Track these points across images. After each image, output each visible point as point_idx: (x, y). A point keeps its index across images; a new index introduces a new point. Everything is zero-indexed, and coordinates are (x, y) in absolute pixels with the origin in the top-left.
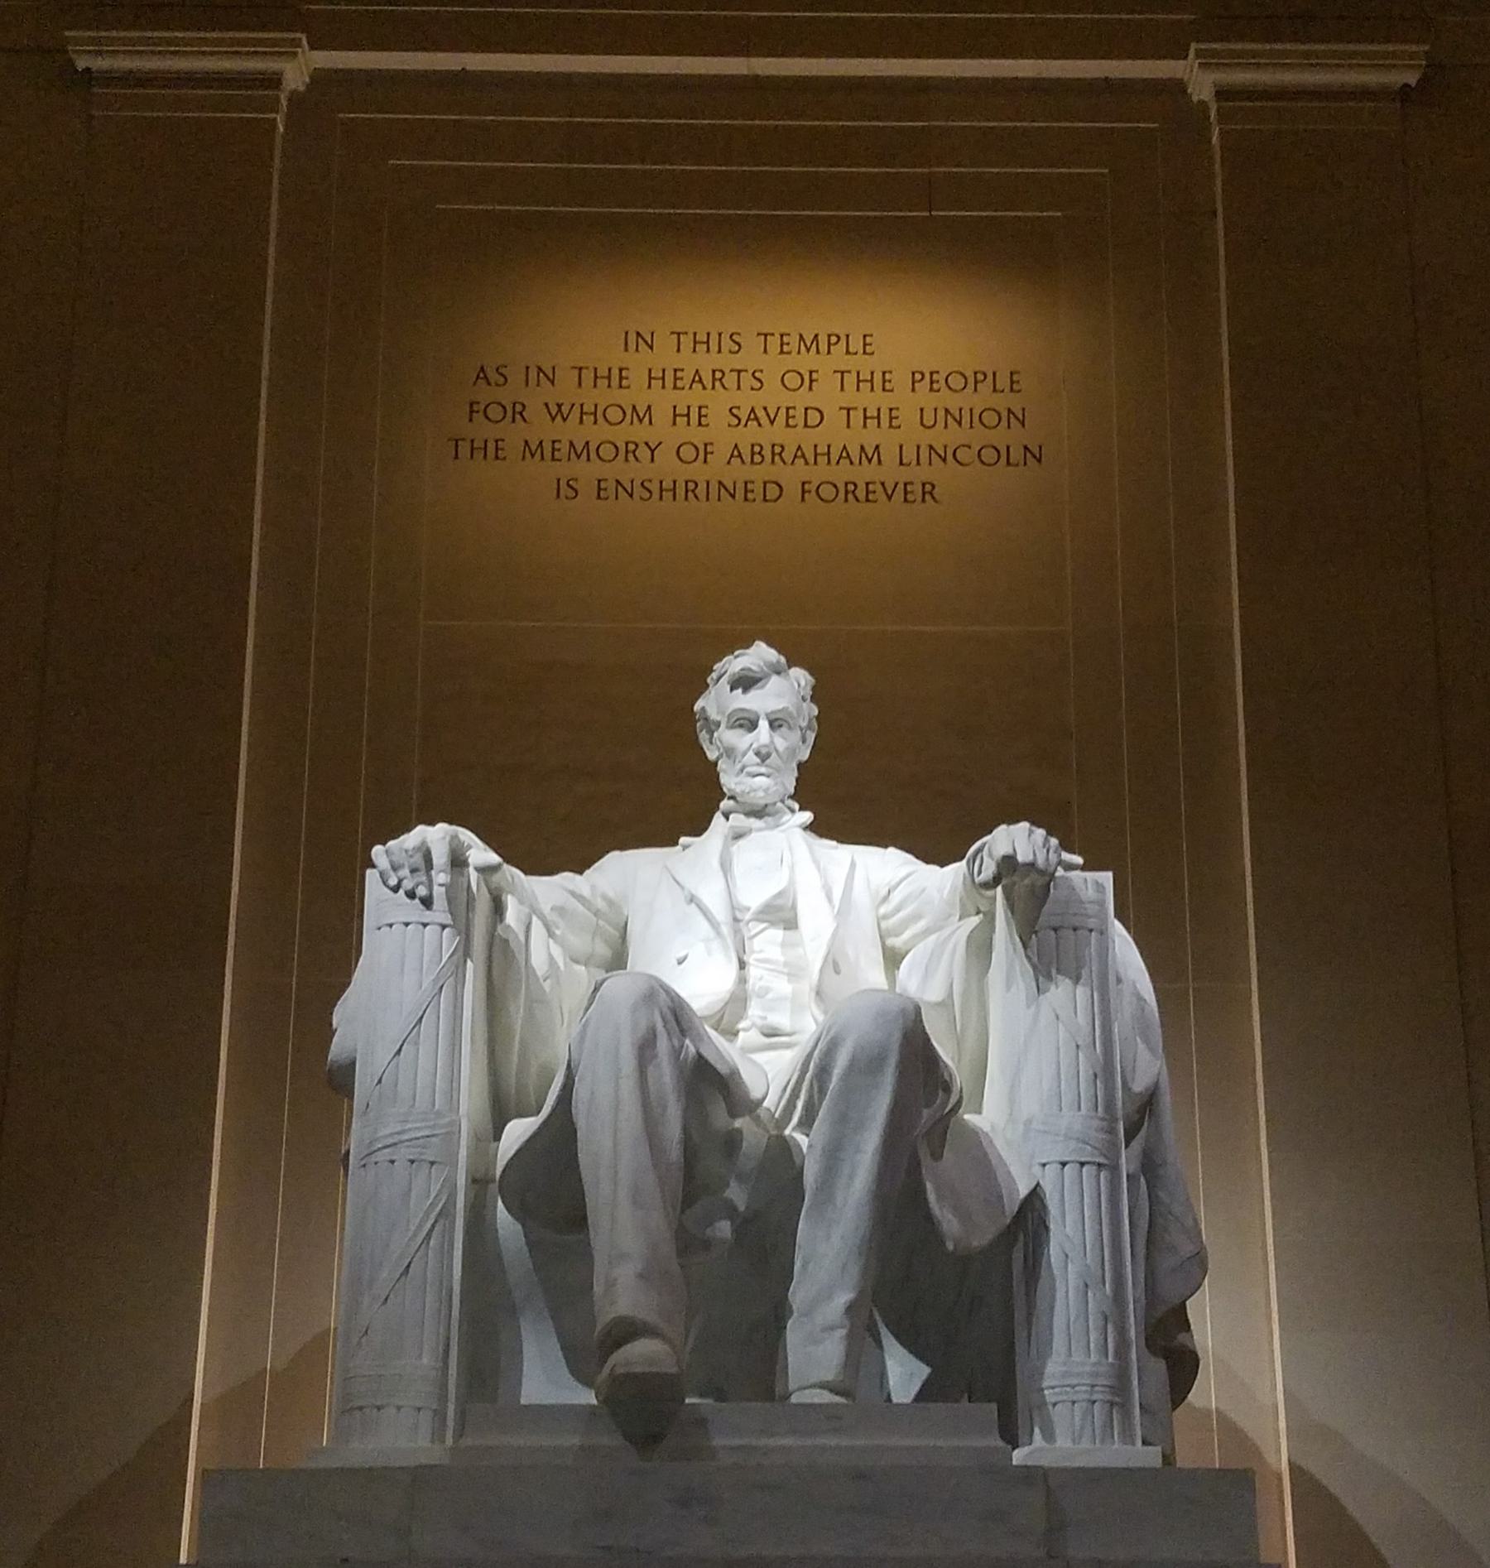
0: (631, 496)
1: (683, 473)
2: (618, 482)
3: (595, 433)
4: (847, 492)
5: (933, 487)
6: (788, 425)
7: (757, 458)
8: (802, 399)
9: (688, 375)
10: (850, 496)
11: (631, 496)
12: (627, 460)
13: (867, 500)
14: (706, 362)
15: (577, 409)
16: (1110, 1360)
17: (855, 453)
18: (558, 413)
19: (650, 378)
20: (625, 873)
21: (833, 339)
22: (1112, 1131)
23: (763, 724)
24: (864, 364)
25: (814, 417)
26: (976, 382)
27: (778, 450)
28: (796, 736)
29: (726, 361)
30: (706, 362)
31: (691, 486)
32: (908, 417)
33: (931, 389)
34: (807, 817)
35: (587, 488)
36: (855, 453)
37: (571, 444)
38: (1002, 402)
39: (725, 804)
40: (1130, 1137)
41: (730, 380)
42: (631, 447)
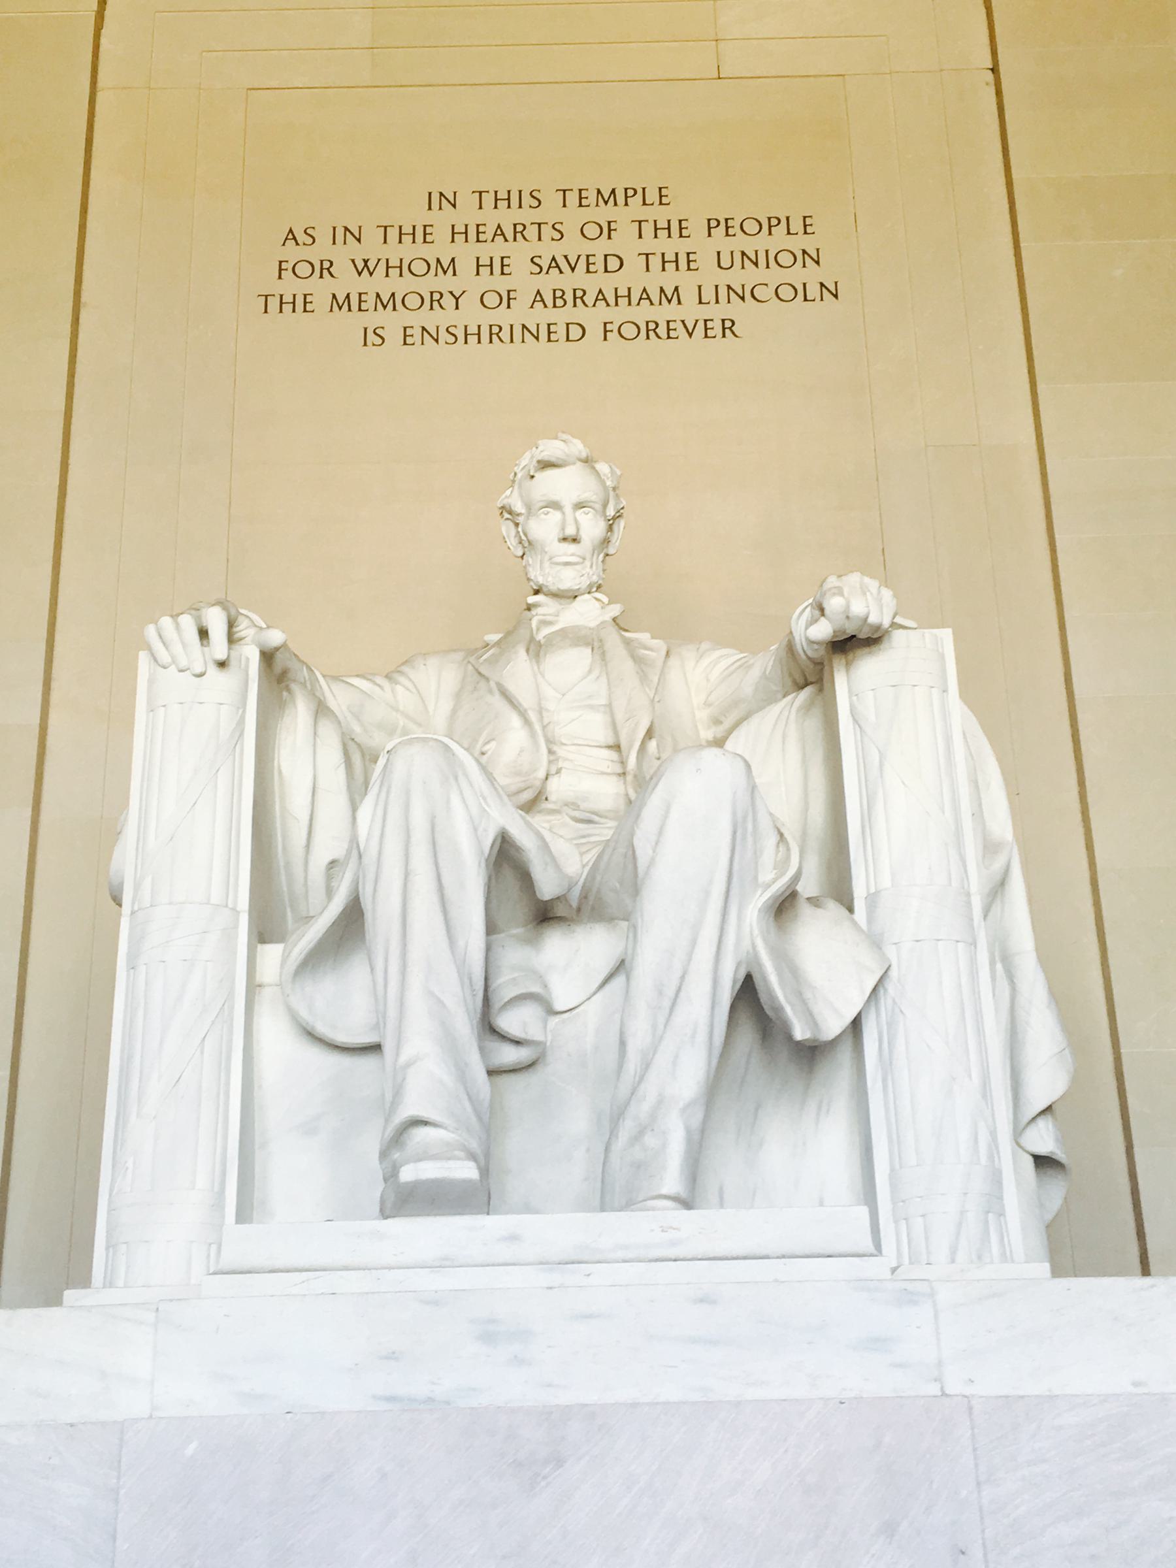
0: (437, 341)
1: (486, 318)
2: (424, 329)
3: (400, 285)
4: (648, 331)
5: (733, 323)
6: (588, 271)
7: (559, 302)
8: (601, 247)
9: (490, 230)
10: (651, 333)
11: (437, 341)
12: (432, 308)
13: (669, 337)
14: (507, 217)
15: (383, 264)
16: (984, 1160)
17: (655, 298)
18: (365, 268)
19: (453, 233)
21: (631, 193)
22: (969, 904)
23: (568, 509)
24: (661, 215)
25: (613, 264)
26: (770, 227)
27: (579, 294)
28: (602, 525)
29: (526, 216)
30: (507, 217)
31: (495, 330)
32: (705, 260)
33: (727, 235)
34: (615, 610)
35: (394, 336)
36: (655, 298)
37: (378, 295)
38: (798, 243)
39: (532, 599)
40: (985, 917)
41: (531, 232)
42: (436, 296)
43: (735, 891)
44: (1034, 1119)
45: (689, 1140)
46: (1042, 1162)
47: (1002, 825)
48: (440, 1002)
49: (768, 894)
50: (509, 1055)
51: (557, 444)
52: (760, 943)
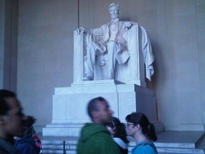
16: (136, 72)
20: (103, 27)
22: (138, 51)
28: (117, 11)
43: (114, 53)
44: (149, 66)
45: (111, 72)
46: (150, 70)
47: (146, 41)
48: (89, 65)
49: (117, 52)
50: (102, 65)
51: (112, 4)
52: (116, 57)
